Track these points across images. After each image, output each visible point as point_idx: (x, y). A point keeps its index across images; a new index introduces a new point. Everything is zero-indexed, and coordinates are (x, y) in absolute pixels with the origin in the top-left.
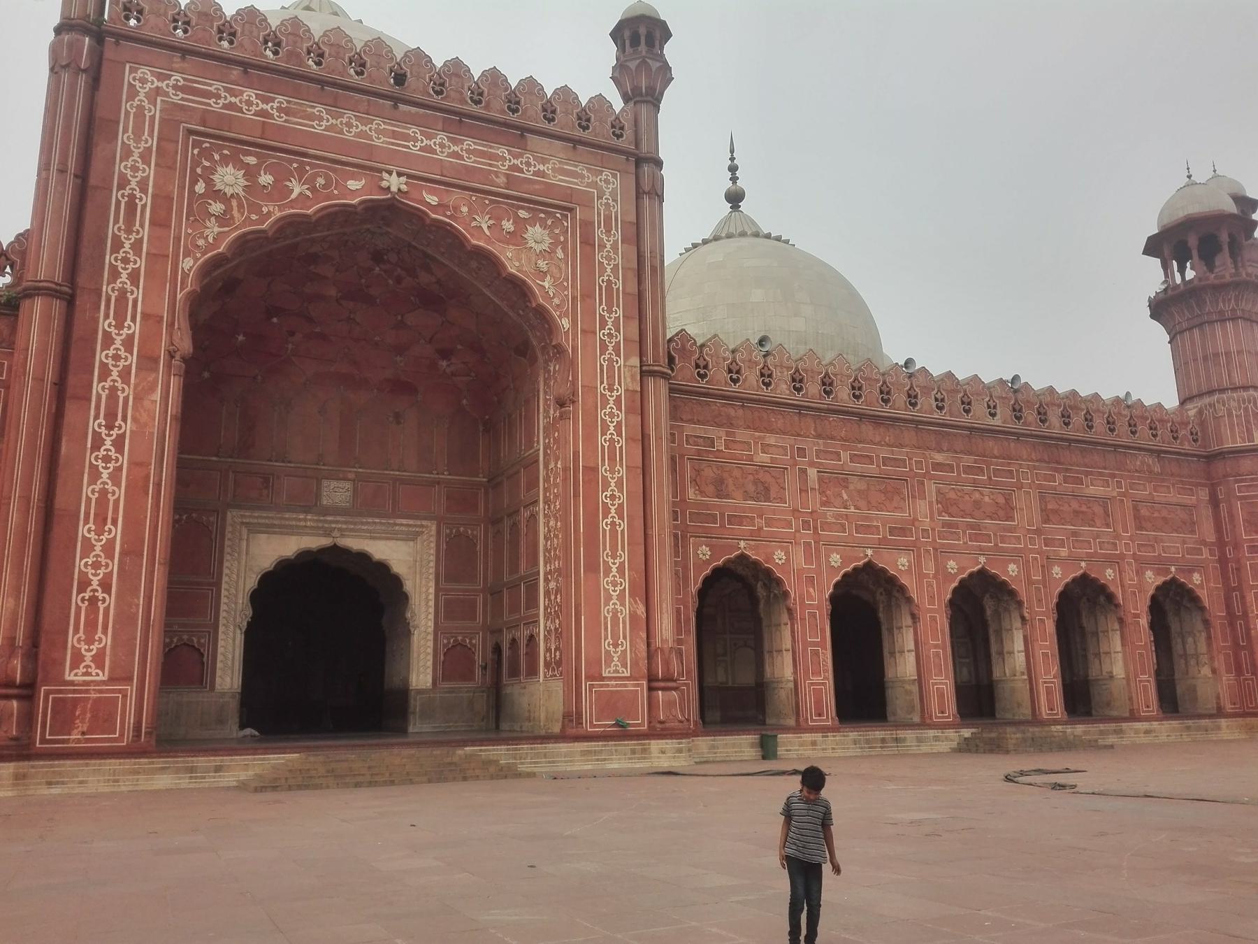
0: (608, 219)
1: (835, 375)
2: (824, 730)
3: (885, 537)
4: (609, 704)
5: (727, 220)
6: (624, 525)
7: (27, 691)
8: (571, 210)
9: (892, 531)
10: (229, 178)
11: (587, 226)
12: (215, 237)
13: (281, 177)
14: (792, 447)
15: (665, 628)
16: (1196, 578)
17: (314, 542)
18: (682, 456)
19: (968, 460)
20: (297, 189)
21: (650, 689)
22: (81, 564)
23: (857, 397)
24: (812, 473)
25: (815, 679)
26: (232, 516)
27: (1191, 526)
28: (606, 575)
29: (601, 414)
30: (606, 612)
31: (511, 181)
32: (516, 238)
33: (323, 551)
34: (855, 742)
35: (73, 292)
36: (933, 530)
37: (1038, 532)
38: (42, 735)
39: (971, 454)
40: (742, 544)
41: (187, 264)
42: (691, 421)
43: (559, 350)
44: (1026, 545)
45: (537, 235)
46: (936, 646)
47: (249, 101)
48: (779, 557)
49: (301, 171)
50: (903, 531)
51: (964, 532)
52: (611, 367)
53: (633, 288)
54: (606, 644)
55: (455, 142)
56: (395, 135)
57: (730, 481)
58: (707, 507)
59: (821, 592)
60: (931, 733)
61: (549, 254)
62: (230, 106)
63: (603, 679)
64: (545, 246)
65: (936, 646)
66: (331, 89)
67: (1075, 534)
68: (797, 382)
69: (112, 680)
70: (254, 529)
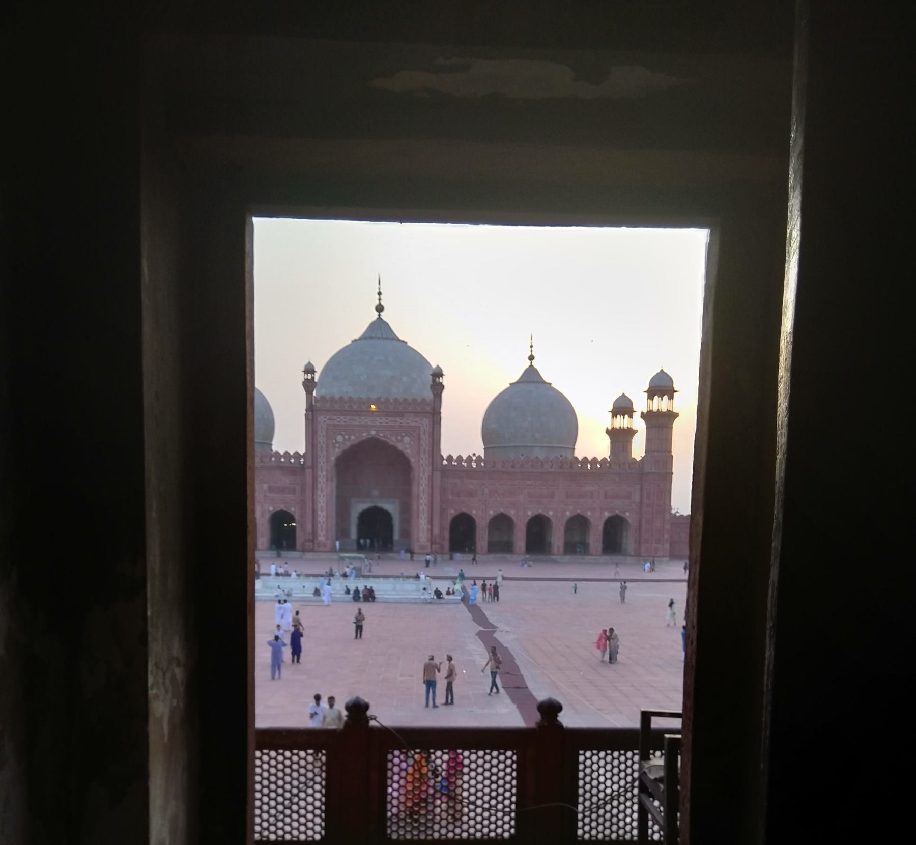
7: (313, 541)
10: (340, 438)
11: (419, 435)
12: (338, 451)
13: (349, 435)
15: (436, 531)
16: (627, 514)
20: (353, 438)
22: (319, 519)
24: (486, 490)
31: (400, 427)
32: (402, 441)
38: (316, 548)
41: (333, 458)
48: (474, 512)
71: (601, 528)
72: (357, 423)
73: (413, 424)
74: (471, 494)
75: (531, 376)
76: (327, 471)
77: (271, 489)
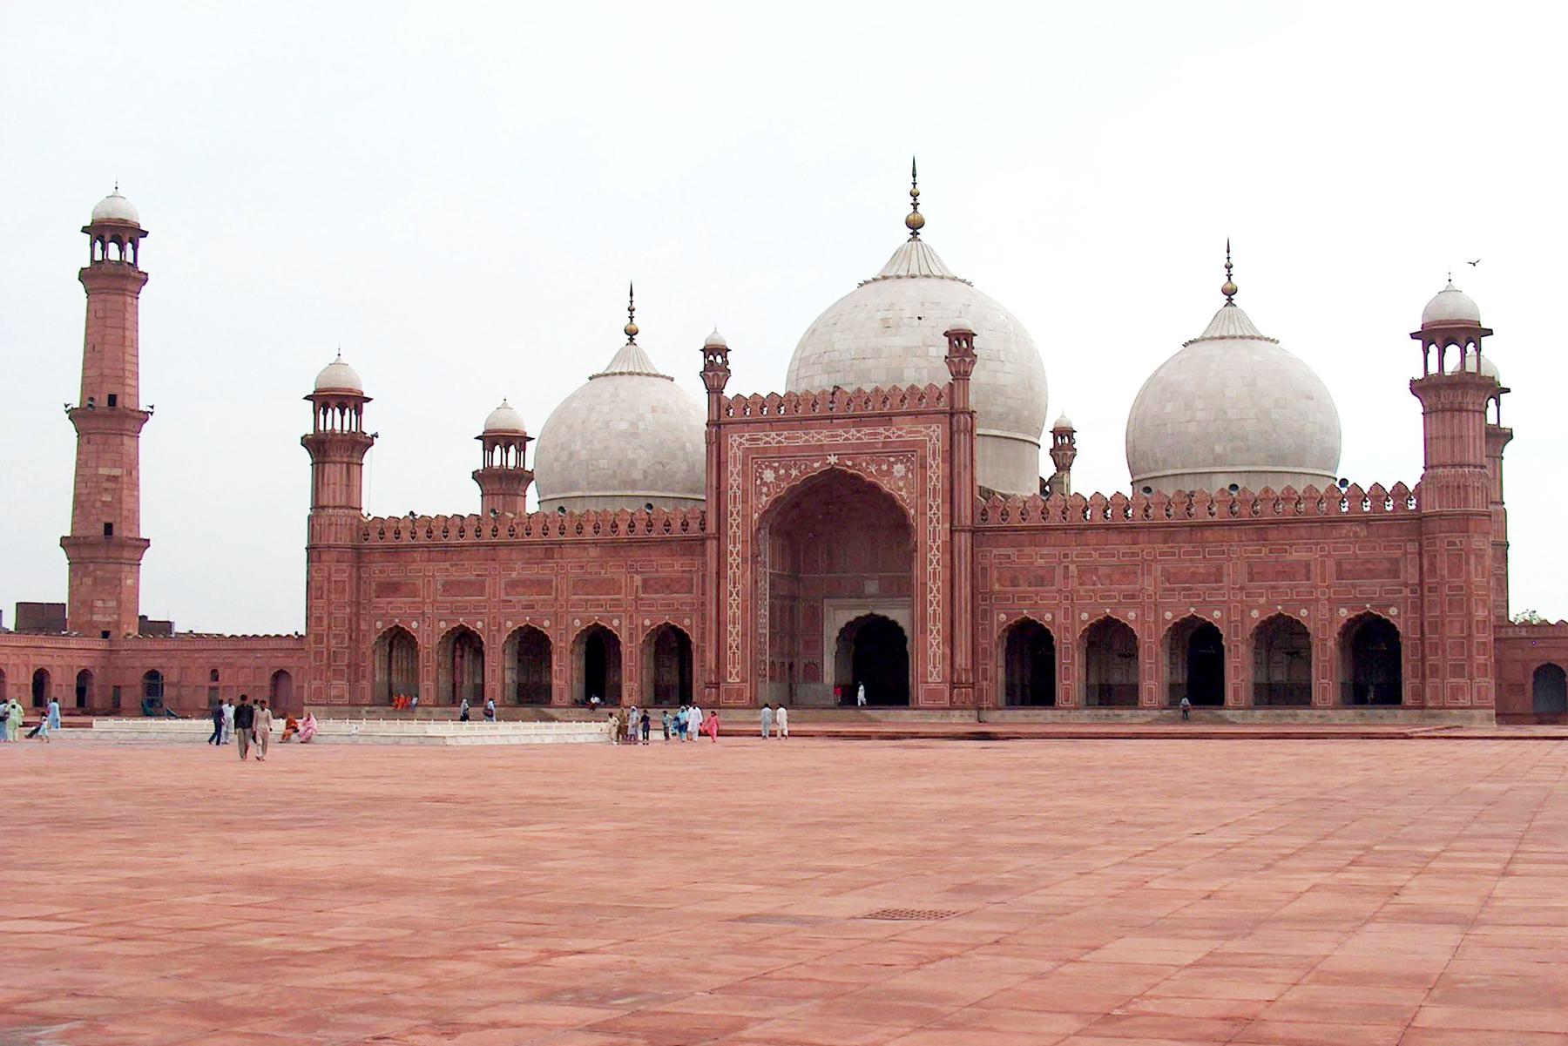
4: (934, 694)
10: (769, 475)
15: (962, 660)
16: (1393, 611)
17: (863, 613)
19: (1188, 547)
21: (953, 687)
24: (1072, 568)
27: (1394, 573)
30: (930, 652)
32: (889, 472)
33: (867, 617)
35: (719, 535)
37: (1242, 588)
41: (756, 516)
43: (910, 526)
45: (899, 469)
47: (772, 438)
48: (1048, 617)
50: (1133, 597)
53: (947, 487)
54: (930, 667)
66: (805, 422)
67: (1273, 588)
70: (836, 608)
71: (1331, 643)
75: (1230, 327)
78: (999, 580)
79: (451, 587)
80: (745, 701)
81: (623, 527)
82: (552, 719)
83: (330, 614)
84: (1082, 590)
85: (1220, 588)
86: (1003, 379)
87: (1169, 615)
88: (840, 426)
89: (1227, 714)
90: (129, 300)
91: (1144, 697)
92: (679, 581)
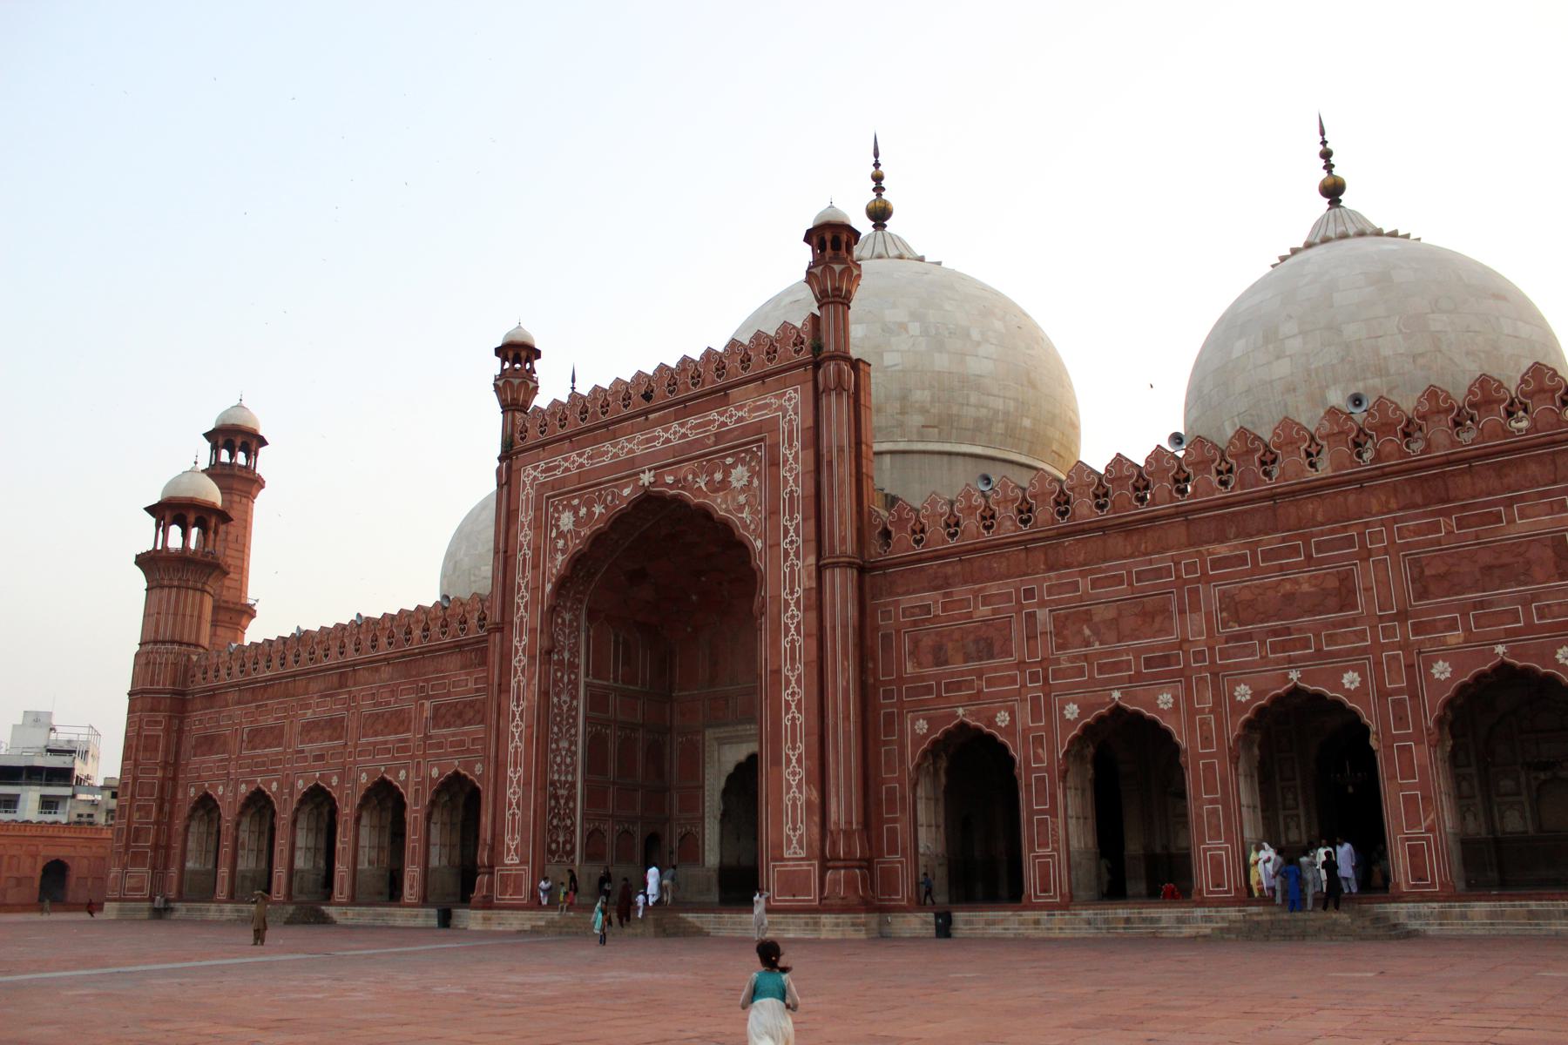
0: (791, 432)
1: (1072, 489)
2: (1050, 907)
3: (1138, 673)
4: (792, 883)
5: (1319, 224)
6: (802, 719)
8: (761, 440)
9: (1149, 663)
10: (567, 521)
11: (775, 447)
13: (589, 504)
14: (1017, 591)
18: (898, 631)
19: (1271, 541)
21: (823, 870)
22: (509, 792)
23: (1101, 507)
24: (1043, 615)
25: (1041, 852)
26: (709, 733)
28: (788, 766)
29: (783, 619)
31: (719, 437)
32: (725, 484)
34: (1089, 922)
36: (1211, 649)
37: (1402, 616)
39: (1276, 530)
40: (960, 711)
41: (548, 587)
42: (907, 593)
44: (1375, 639)
46: (1212, 802)
47: (573, 461)
48: (1003, 719)
49: (600, 496)
51: (1262, 643)
52: (792, 572)
54: (787, 829)
55: (682, 425)
56: (648, 441)
57: (950, 645)
58: (922, 678)
59: (1051, 752)
60: (1199, 912)
61: (747, 488)
62: (567, 469)
63: (782, 859)
64: (742, 483)
65: (1212, 802)
68: (1025, 512)
69: (521, 863)
70: (722, 742)
72: (607, 460)
73: (756, 417)
74: (987, 644)
76: (533, 631)
77: (438, 717)
78: (914, 653)
79: (258, 736)
80: (523, 897)
81: (417, 633)
82: (325, 920)
83: (135, 779)
84: (1064, 659)
85: (1355, 621)
86: (974, 366)
87: (1243, 692)
88: (658, 423)
89: (1400, 911)
90: (237, 498)
91: (1203, 878)
92: (471, 704)
